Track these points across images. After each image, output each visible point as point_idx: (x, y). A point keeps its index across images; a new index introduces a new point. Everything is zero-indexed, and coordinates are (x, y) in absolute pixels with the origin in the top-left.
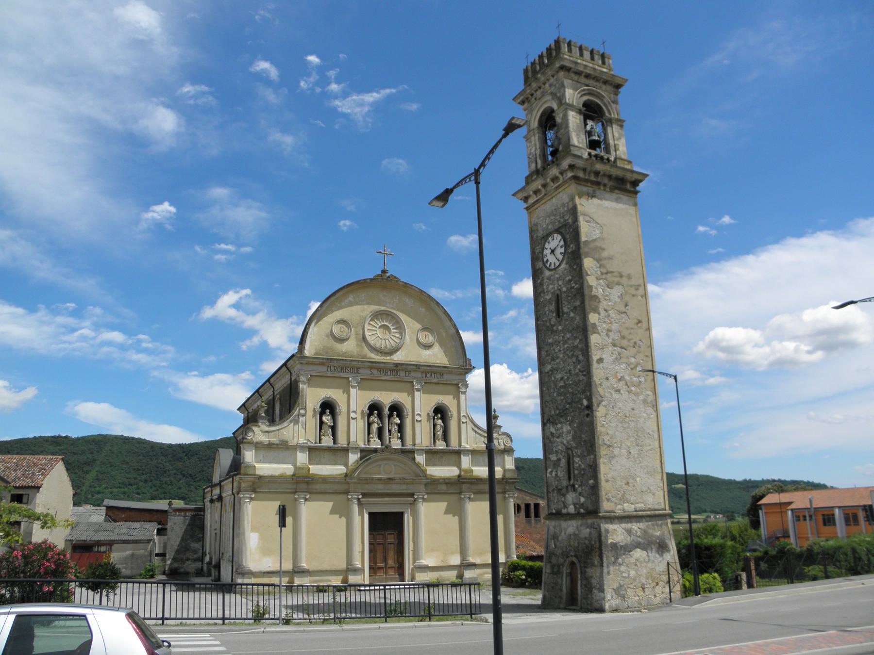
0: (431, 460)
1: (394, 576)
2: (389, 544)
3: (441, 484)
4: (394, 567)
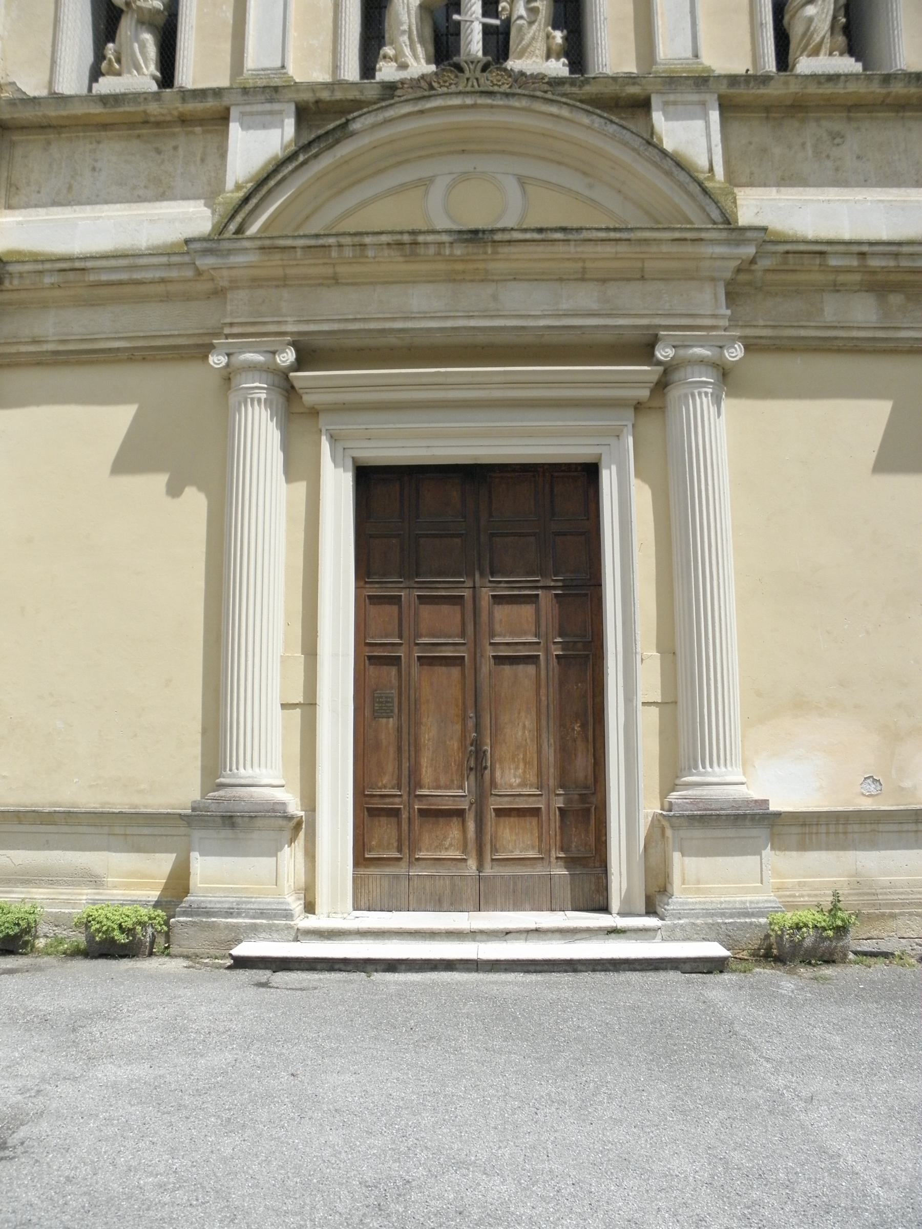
0: (764, 150)
1: (539, 870)
2: (500, 660)
3: (836, 288)
4: (535, 812)
